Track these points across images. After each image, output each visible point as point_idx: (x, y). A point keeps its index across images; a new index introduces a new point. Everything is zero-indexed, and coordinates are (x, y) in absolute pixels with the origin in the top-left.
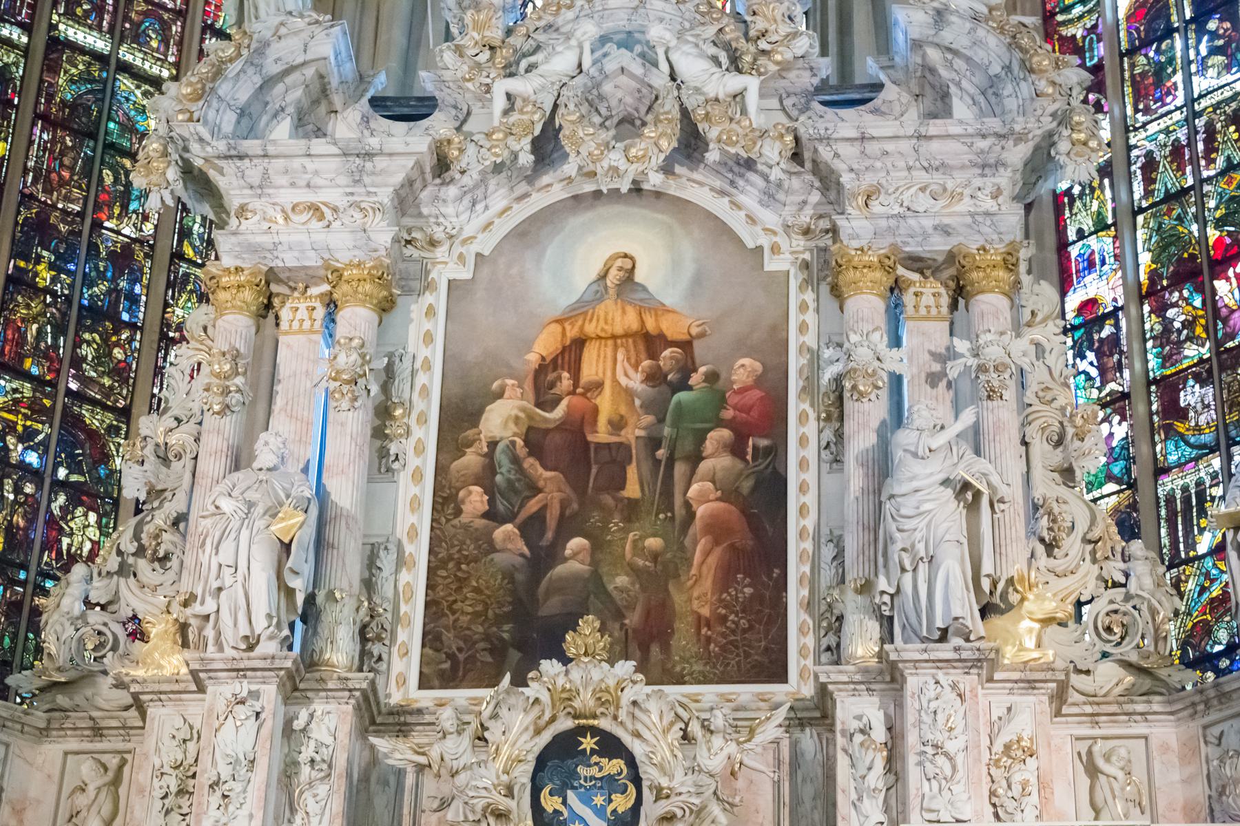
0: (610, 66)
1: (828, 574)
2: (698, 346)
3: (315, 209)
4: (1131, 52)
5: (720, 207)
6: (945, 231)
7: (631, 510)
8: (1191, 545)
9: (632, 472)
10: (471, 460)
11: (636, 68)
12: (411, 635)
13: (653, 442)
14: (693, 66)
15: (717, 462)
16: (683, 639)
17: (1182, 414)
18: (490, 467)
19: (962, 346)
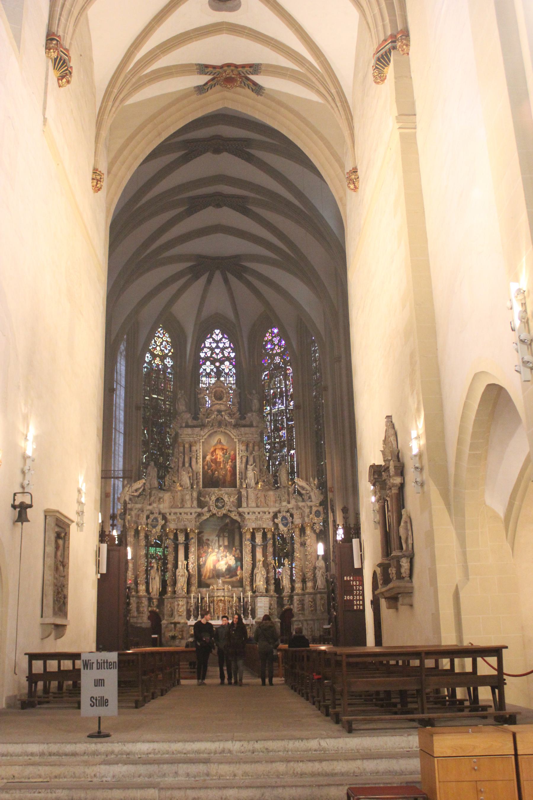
0: (218, 416)
1: (241, 477)
2: (228, 450)
3: (188, 435)
4: (273, 399)
5: (230, 433)
6: (252, 439)
7: (222, 469)
8: (276, 463)
9: (222, 465)
10: (205, 463)
11: (221, 417)
12: (201, 483)
13: (223, 461)
14: (227, 418)
15: (230, 463)
16: (227, 483)
17: (276, 447)
18: (207, 464)
19: (254, 452)
